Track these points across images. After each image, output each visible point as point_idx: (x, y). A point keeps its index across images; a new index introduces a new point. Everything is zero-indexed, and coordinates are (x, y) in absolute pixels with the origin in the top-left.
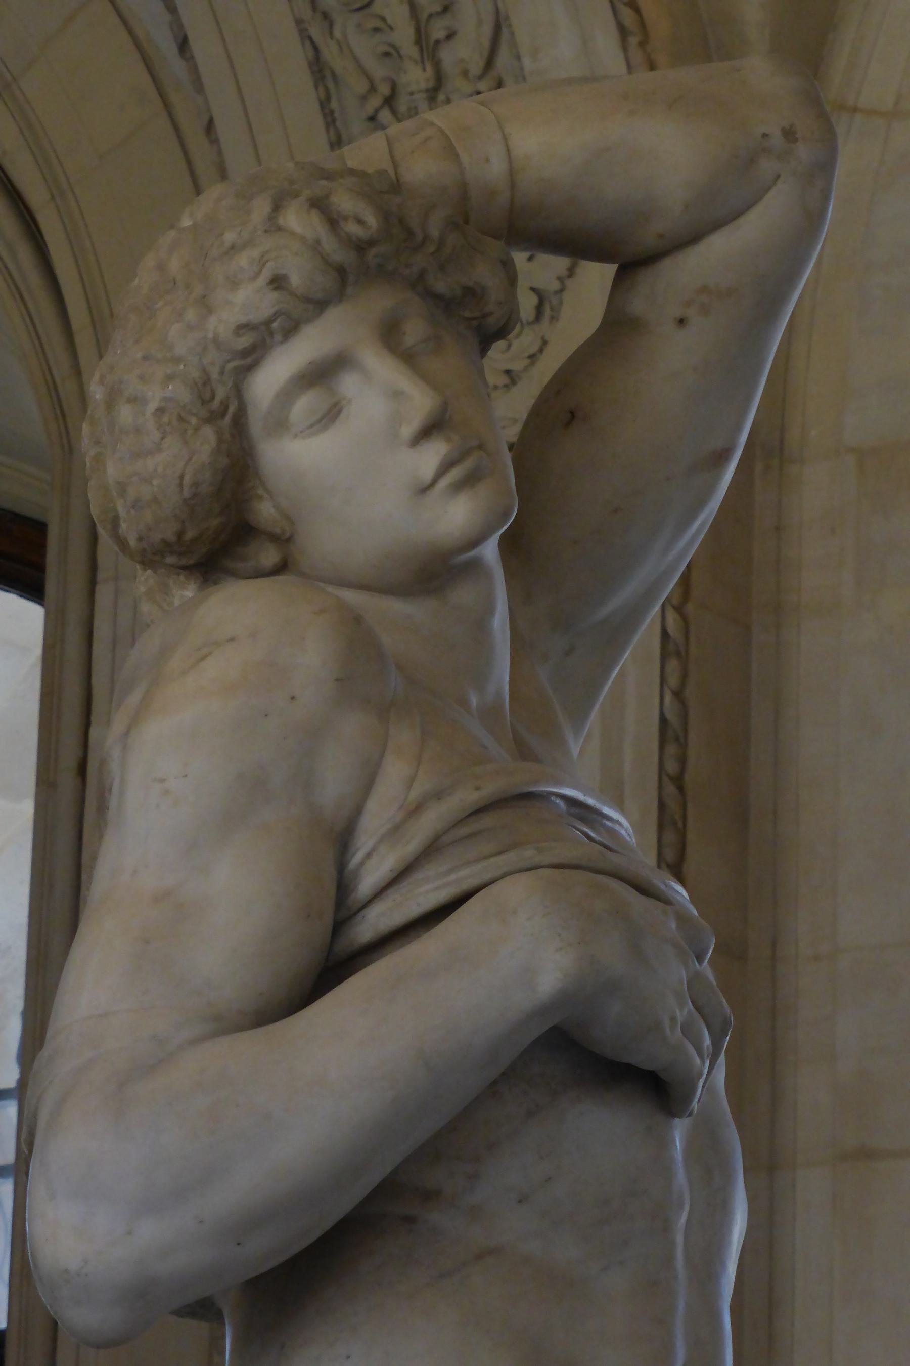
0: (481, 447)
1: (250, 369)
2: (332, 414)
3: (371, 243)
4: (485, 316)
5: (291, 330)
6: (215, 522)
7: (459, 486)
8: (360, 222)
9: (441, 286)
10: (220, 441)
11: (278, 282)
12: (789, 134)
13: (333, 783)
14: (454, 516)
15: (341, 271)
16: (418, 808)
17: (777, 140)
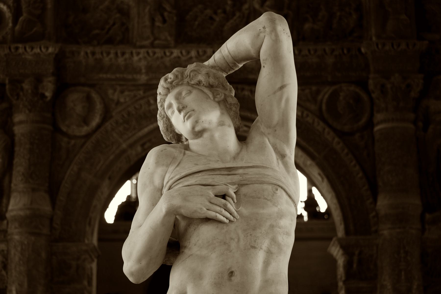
0: (193, 110)
1: (164, 109)
2: (173, 112)
3: (173, 81)
4: (204, 84)
5: (164, 101)
6: (171, 135)
7: (187, 119)
8: (171, 78)
9: (192, 82)
10: (163, 122)
11: (160, 94)
12: (264, 28)
13: (157, 181)
14: (189, 124)
15: (168, 89)
16: (168, 182)
17: (262, 29)
